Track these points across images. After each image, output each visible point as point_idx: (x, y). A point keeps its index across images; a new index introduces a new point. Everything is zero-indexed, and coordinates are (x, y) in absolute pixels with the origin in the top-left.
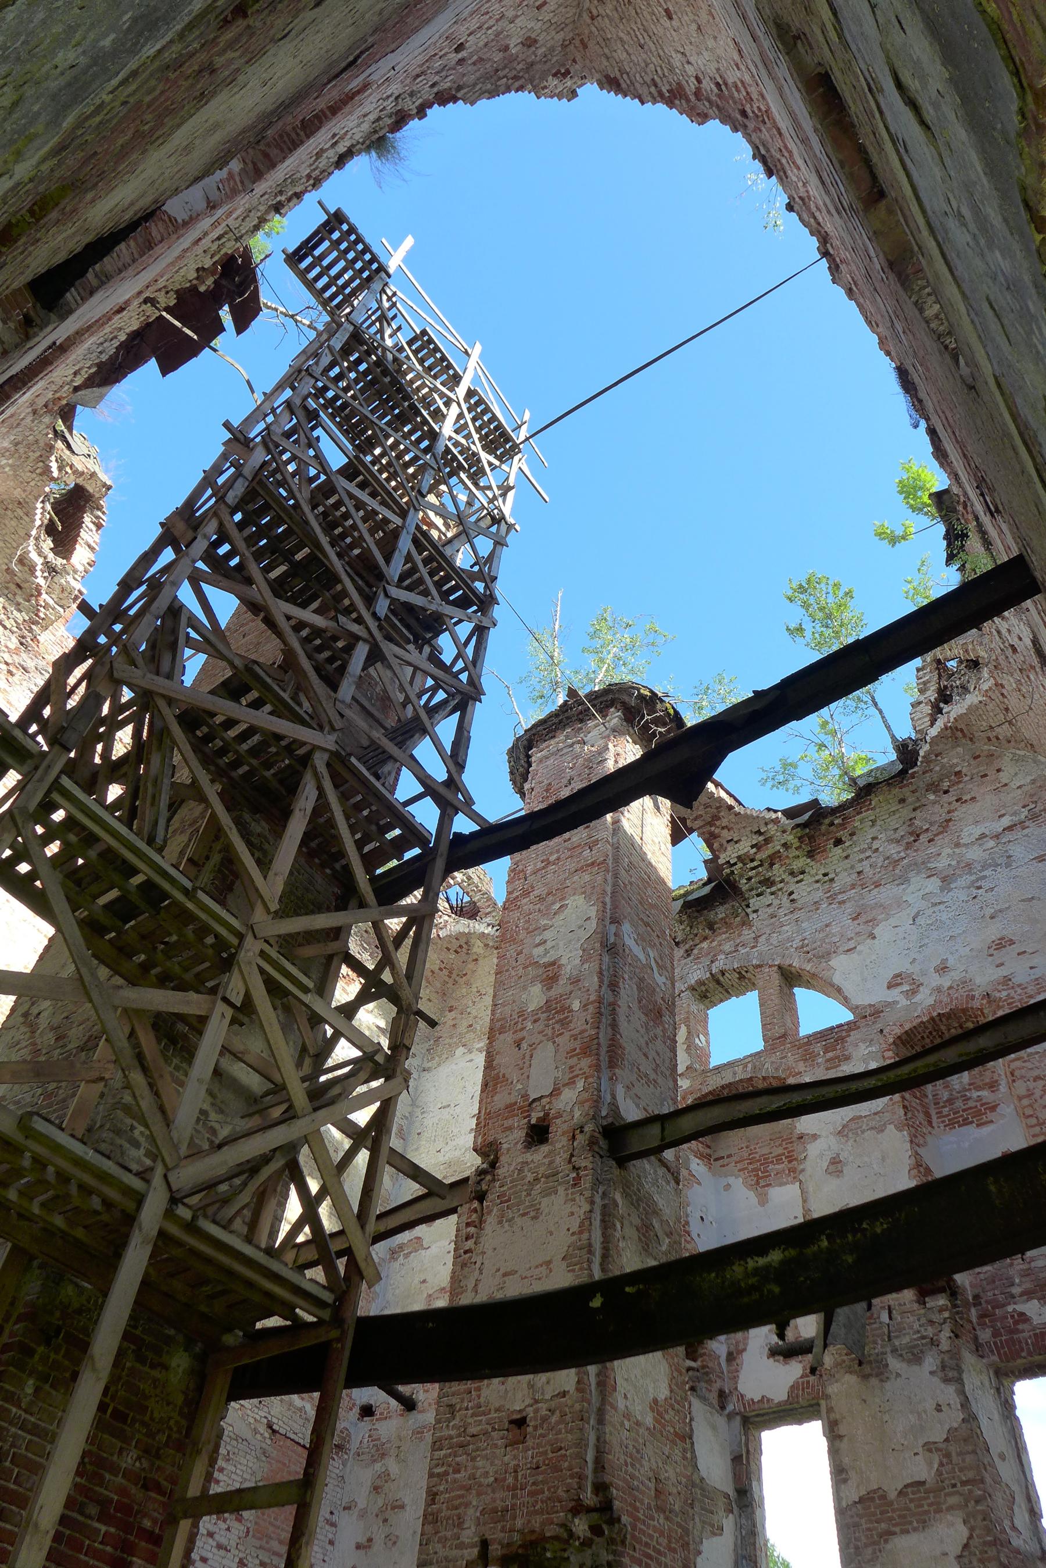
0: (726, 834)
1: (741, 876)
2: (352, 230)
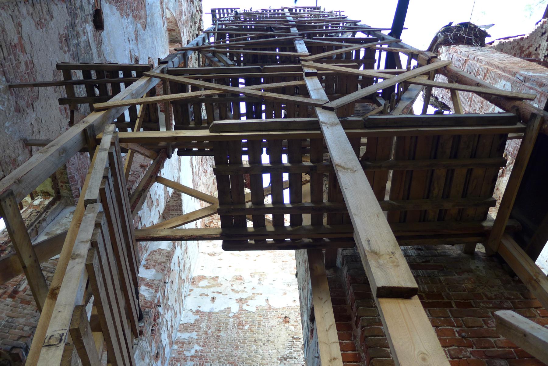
0: (531, 49)
2: (219, 10)
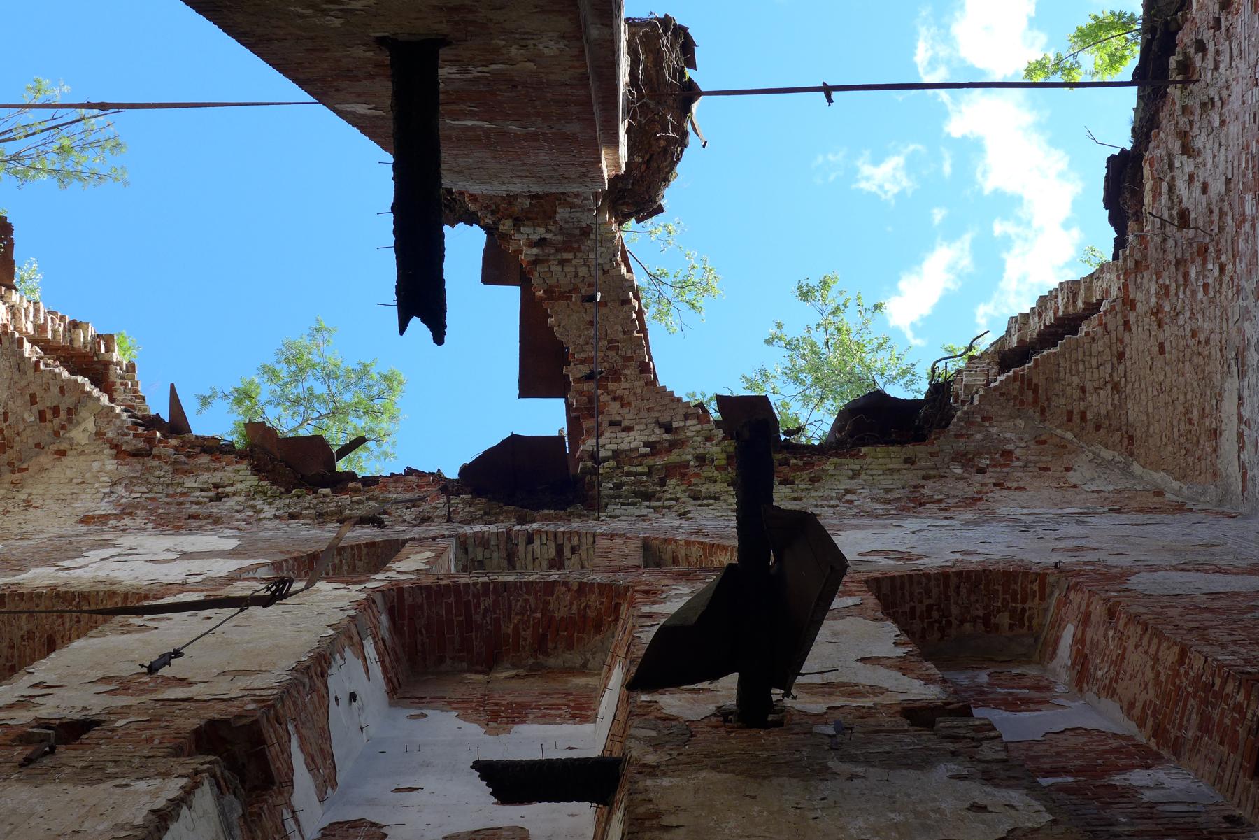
0: (614, 409)
1: (609, 478)
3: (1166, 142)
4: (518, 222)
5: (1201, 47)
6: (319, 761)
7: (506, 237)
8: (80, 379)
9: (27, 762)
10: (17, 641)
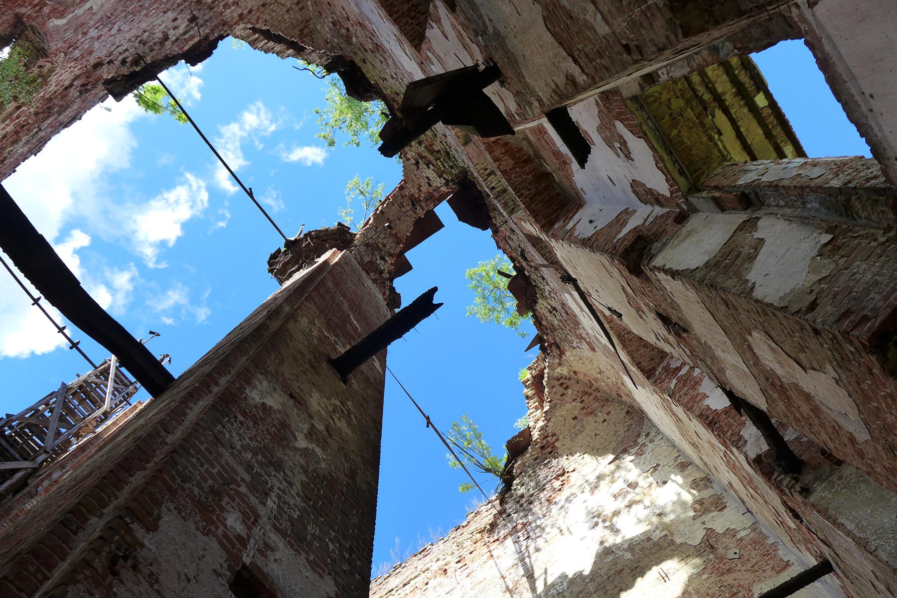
0: (424, 189)
1: (451, 173)
3: (169, 48)
4: (381, 272)
5: (124, 62)
6: (622, 221)
7: (390, 272)
8: (545, 384)
9: (685, 331)
10: (650, 349)
